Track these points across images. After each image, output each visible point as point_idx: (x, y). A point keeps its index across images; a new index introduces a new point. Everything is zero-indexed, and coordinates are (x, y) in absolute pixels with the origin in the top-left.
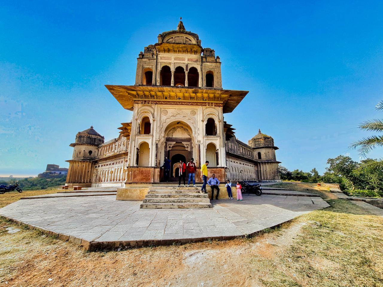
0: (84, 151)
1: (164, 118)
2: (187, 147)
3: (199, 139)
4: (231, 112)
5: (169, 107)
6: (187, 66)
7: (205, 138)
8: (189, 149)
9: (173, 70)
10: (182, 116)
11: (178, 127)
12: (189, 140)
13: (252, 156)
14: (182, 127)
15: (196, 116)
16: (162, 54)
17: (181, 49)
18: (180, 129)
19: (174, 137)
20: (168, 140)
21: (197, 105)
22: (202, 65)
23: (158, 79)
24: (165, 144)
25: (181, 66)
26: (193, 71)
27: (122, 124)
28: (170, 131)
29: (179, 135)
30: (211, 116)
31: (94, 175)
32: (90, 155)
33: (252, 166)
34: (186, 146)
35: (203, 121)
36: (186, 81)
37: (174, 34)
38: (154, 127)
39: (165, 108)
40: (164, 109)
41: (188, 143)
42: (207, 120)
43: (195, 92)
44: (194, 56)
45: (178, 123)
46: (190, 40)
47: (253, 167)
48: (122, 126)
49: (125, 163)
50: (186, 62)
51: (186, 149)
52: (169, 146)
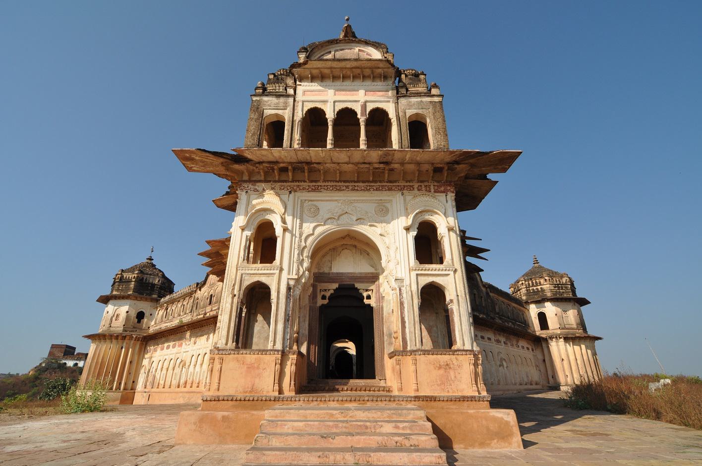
0: (127, 312)
3: (399, 276)
4: (474, 207)
5: (323, 199)
6: (364, 107)
9: (330, 115)
10: (355, 218)
11: (345, 247)
13: (526, 323)
14: (355, 247)
16: (306, 84)
17: (349, 73)
18: (349, 251)
19: (335, 270)
20: (319, 278)
21: (390, 189)
22: (398, 103)
23: (297, 136)
24: (311, 289)
25: (350, 107)
27: (208, 242)
28: (324, 256)
29: (347, 266)
31: (142, 371)
32: (139, 322)
33: (528, 349)
36: (361, 139)
37: (334, 46)
38: (285, 247)
39: (311, 201)
40: (310, 203)
42: (417, 226)
43: (385, 160)
45: (343, 238)
47: (531, 350)
48: (208, 248)
51: (366, 301)
52: (323, 293)
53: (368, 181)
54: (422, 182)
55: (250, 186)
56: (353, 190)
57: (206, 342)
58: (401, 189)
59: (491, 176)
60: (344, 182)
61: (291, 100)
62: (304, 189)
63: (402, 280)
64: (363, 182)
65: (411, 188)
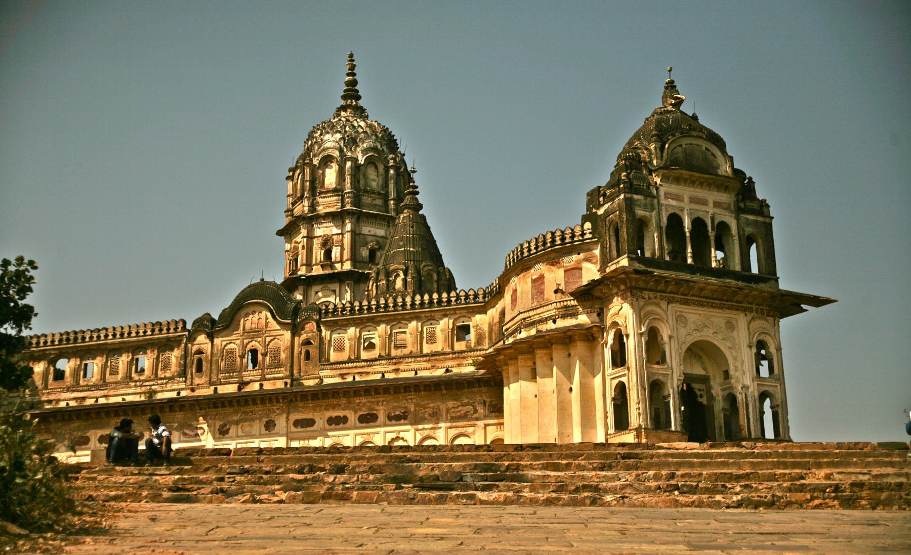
1: (683, 332)
2: (701, 396)
7: (756, 383)
8: (704, 401)
10: (711, 331)
12: (705, 380)
15: (735, 333)
21: (737, 309)
26: (722, 228)
30: (762, 337)
34: (698, 393)
35: (750, 347)
41: (703, 387)
44: (724, 198)
46: (713, 155)
49: (293, 429)
50: (711, 210)
51: (700, 400)
53: (722, 300)
54: (757, 305)
55: (639, 294)
56: (712, 306)
57: (263, 431)
58: (745, 310)
59: (804, 306)
60: (706, 298)
61: (656, 200)
62: (677, 301)
63: (748, 388)
64: (719, 300)
65: (751, 310)
